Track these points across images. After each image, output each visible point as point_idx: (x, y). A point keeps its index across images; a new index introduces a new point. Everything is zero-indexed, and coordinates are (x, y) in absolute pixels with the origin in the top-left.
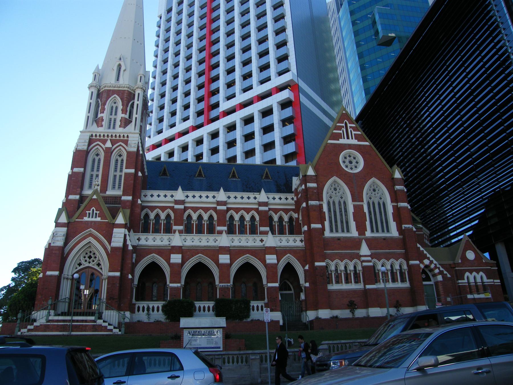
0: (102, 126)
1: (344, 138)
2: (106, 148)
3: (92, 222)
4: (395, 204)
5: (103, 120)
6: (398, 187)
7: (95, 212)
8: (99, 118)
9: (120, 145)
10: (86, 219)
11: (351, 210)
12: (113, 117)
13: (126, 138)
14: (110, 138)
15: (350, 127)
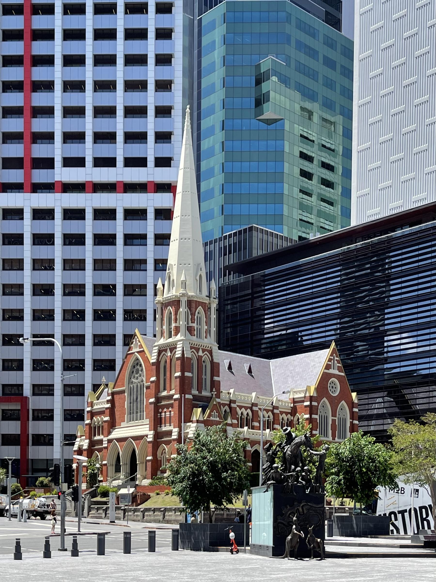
0: (194, 335)
1: (334, 369)
2: (198, 356)
3: (215, 421)
4: (351, 420)
5: (195, 330)
6: (355, 410)
7: (216, 413)
8: (191, 327)
9: (206, 354)
10: (211, 418)
11: (330, 422)
12: (199, 327)
13: (209, 349)
14: (200, 347)
15: (336, 360)
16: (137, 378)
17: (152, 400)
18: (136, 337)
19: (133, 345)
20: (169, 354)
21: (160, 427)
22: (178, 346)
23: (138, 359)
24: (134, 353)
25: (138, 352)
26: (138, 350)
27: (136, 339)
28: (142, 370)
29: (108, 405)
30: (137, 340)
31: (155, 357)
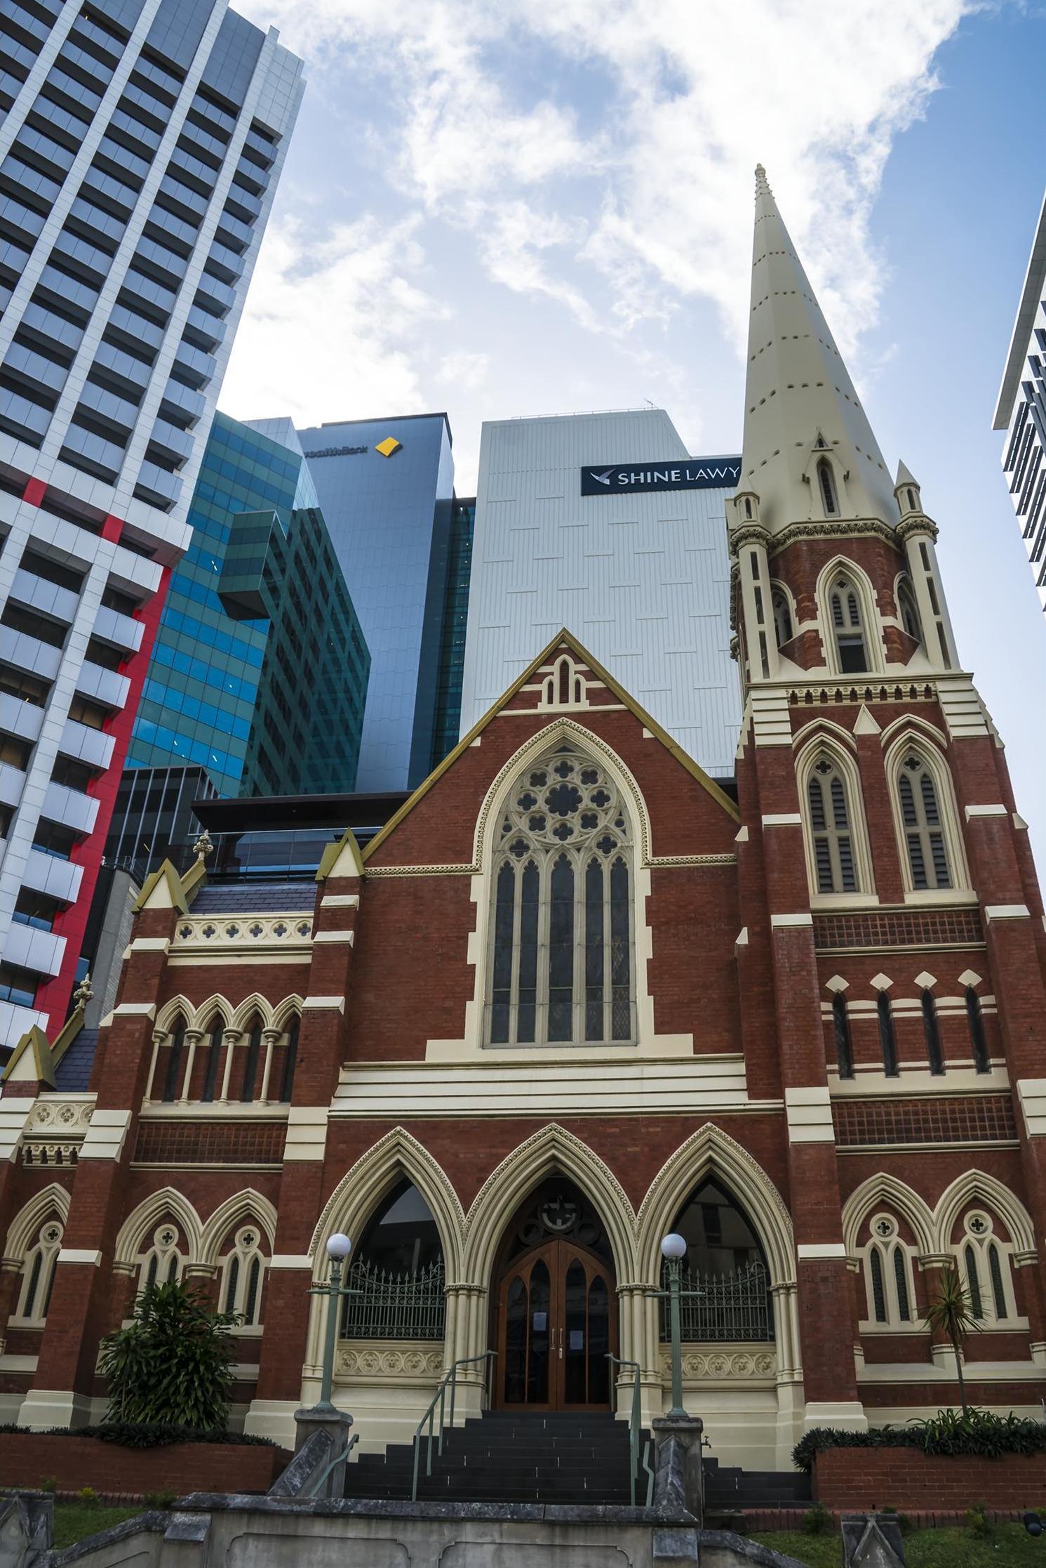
16: (563, 832)
17: (805, 919)
18: (564, 656)
19: (543, 687)
20: (866, 725)
21: (848, 1074)
22: (944, 698)
23: (565, 746)
24: (552, 717)
25: (579, 717)
26: (585, 706)
27: (564, 666)
28: (601, 799)
29: (346, 936)
30: (573, 667)
31: (787, 728)
